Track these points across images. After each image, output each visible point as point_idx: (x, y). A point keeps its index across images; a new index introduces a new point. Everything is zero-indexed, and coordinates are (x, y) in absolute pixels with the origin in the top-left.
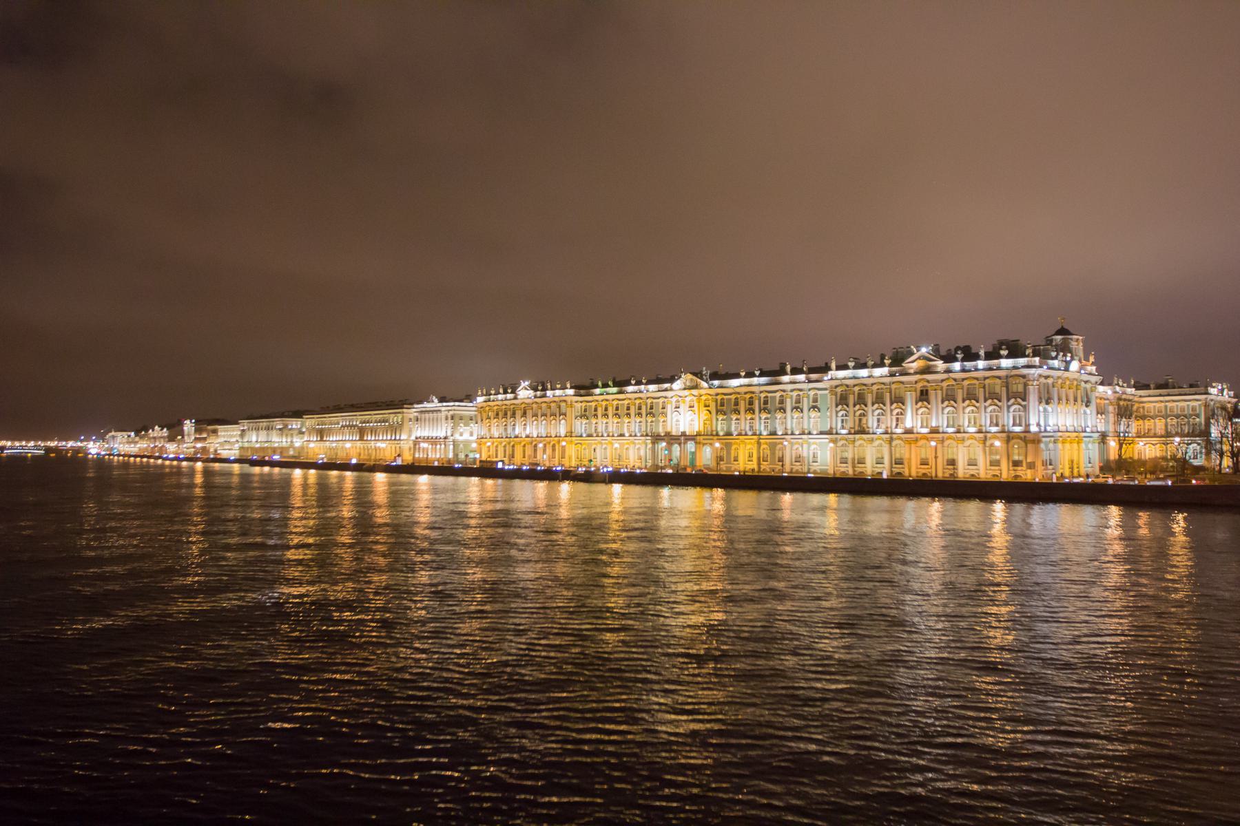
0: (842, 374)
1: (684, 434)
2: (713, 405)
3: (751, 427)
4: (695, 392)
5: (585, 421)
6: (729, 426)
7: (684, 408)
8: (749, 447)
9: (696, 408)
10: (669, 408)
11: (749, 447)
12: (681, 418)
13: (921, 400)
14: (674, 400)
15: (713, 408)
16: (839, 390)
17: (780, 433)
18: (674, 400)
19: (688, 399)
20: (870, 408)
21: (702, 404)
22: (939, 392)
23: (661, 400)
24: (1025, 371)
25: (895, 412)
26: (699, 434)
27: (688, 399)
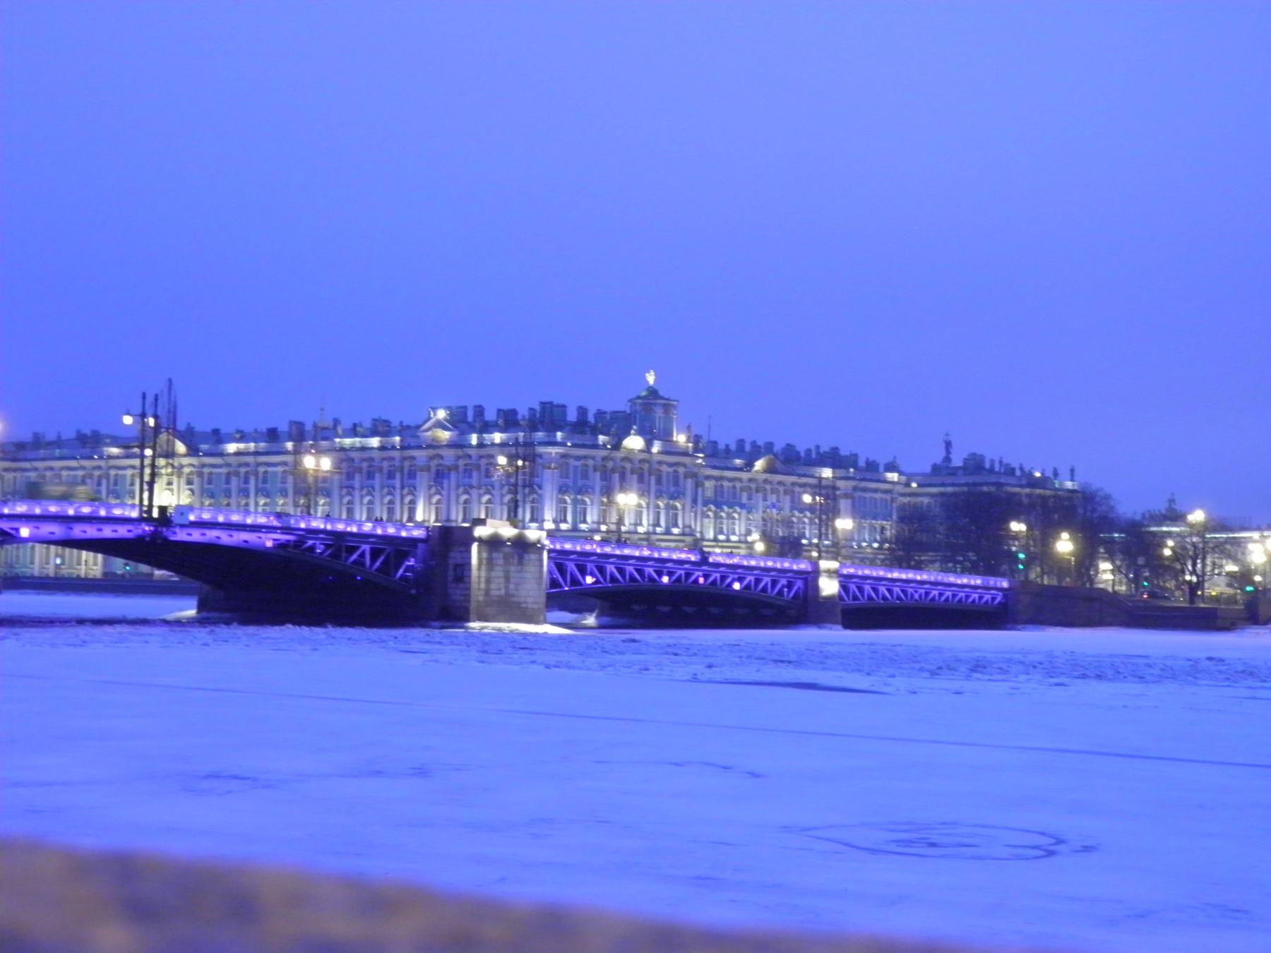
9: (175, 486)
21: (183, 481)
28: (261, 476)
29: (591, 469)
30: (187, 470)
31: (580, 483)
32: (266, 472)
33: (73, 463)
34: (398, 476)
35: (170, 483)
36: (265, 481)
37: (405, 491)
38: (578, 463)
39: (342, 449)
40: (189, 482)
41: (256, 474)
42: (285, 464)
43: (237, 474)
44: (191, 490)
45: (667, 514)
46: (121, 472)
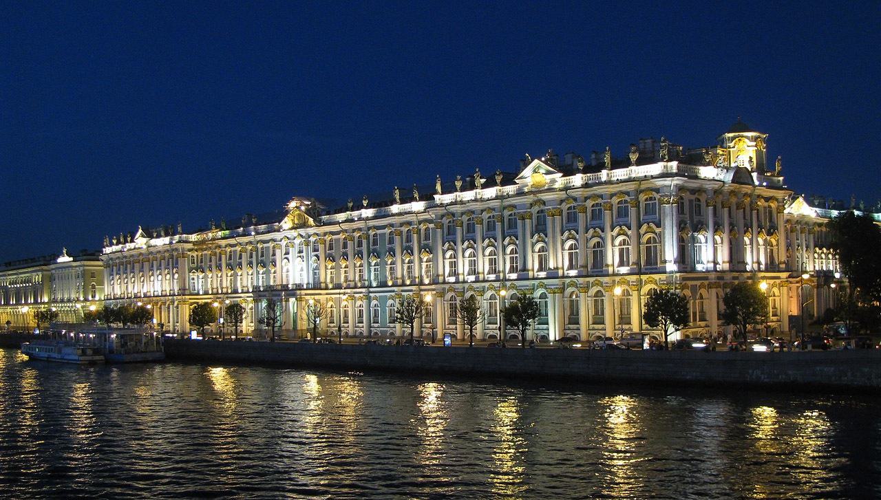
0: (448, 198)
1: (285, 288)
2: (321, 247)
3: (361, 277)
4: (302, 231)
5: (201, 275)
6: (339, 275)
7: (293, 252)
8: (359, 303)
9: (304, 254)
10: (278, 257)
11: (359, 303)
12: (290, 266)
13: (538, 231)
14: (284, 243)
15: (321, 253)
16: (445, 221)
17: (390, 283)
18: (284, 243)
19: (297, 241)
20: (479, 246)
22: (558, 218)
23: (271, 245)
24: (660, 183)
25: (508, 250)
26: (299, 287)
27: (297, 241)
28: (371, 238)
29: (703, 204)
30: (312, 239)
31: (696, 219)
32: (375, 235)
33: (232, 241)
34: (498, 225)
35: (300, 252)
36: (375, 243)
37: (507, 240)
38: (693, 197)
39: (442, 205)
40: (315, 250)
41: (368, 238)
42: (392, 225)
43: (352, 239)
44: (316, 256)
45: (766, 249)
46: (265, 245)
